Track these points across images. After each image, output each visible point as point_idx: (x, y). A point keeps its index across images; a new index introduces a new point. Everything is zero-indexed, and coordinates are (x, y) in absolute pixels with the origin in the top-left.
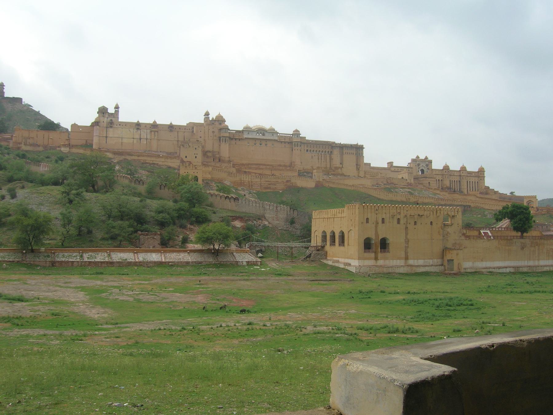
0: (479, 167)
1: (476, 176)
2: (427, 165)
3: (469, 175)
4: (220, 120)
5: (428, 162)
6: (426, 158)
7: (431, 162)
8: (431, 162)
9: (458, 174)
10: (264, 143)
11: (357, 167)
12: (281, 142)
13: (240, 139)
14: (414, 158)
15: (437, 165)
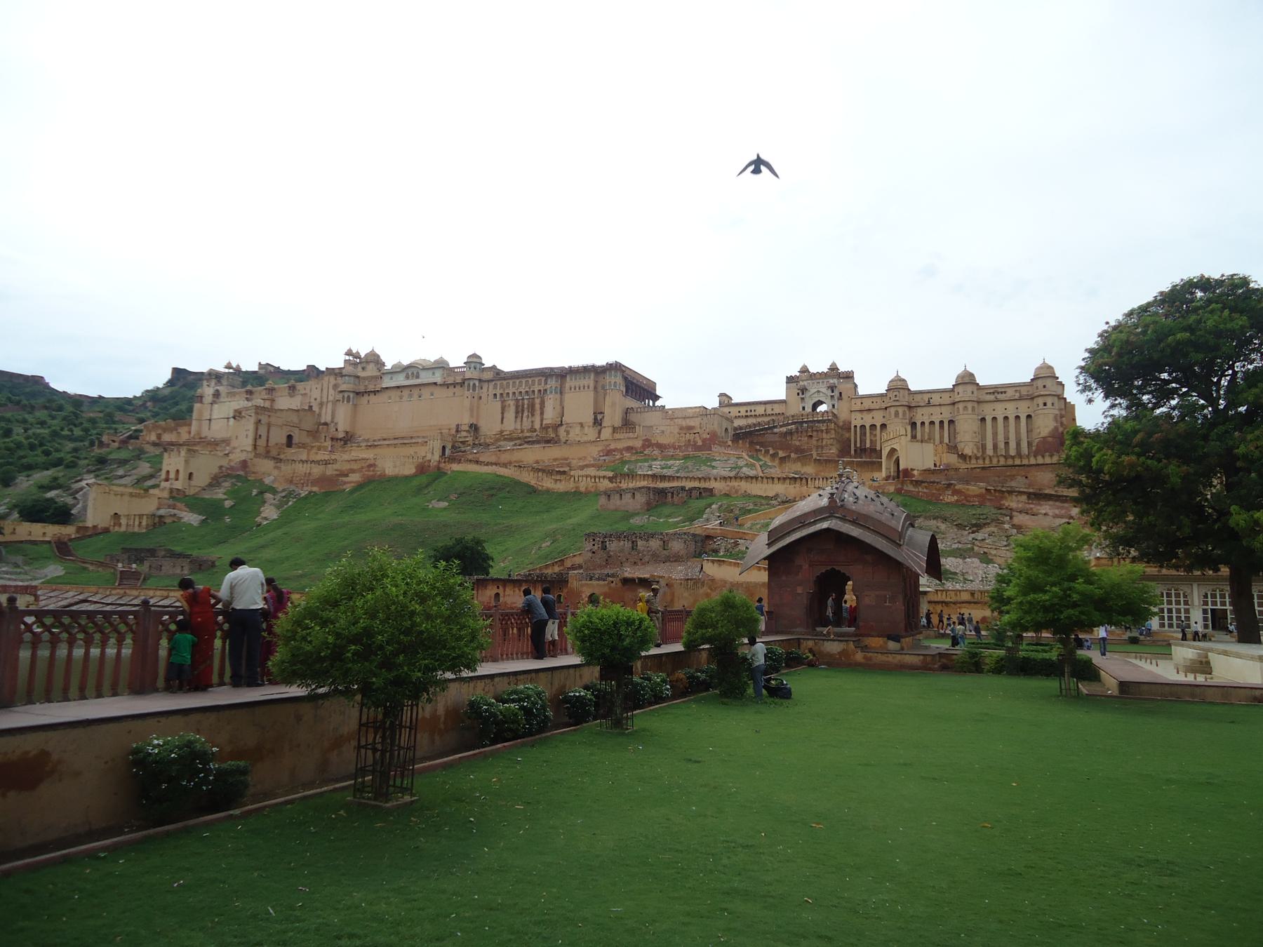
0: (1038, 363)
1: (1021, 399)
2: (832, 388)
3: (992, 397)
4: (374, 359)
5: (838, 379)
6: (833, 368)
7: (849, 376)
8: (849, 376)
9: (946, 399)
10: (416, 392)
11: (595, 419)
12: (448, 386)
13: (375, 392)
14: (795, 373)
15: (871, 383)
